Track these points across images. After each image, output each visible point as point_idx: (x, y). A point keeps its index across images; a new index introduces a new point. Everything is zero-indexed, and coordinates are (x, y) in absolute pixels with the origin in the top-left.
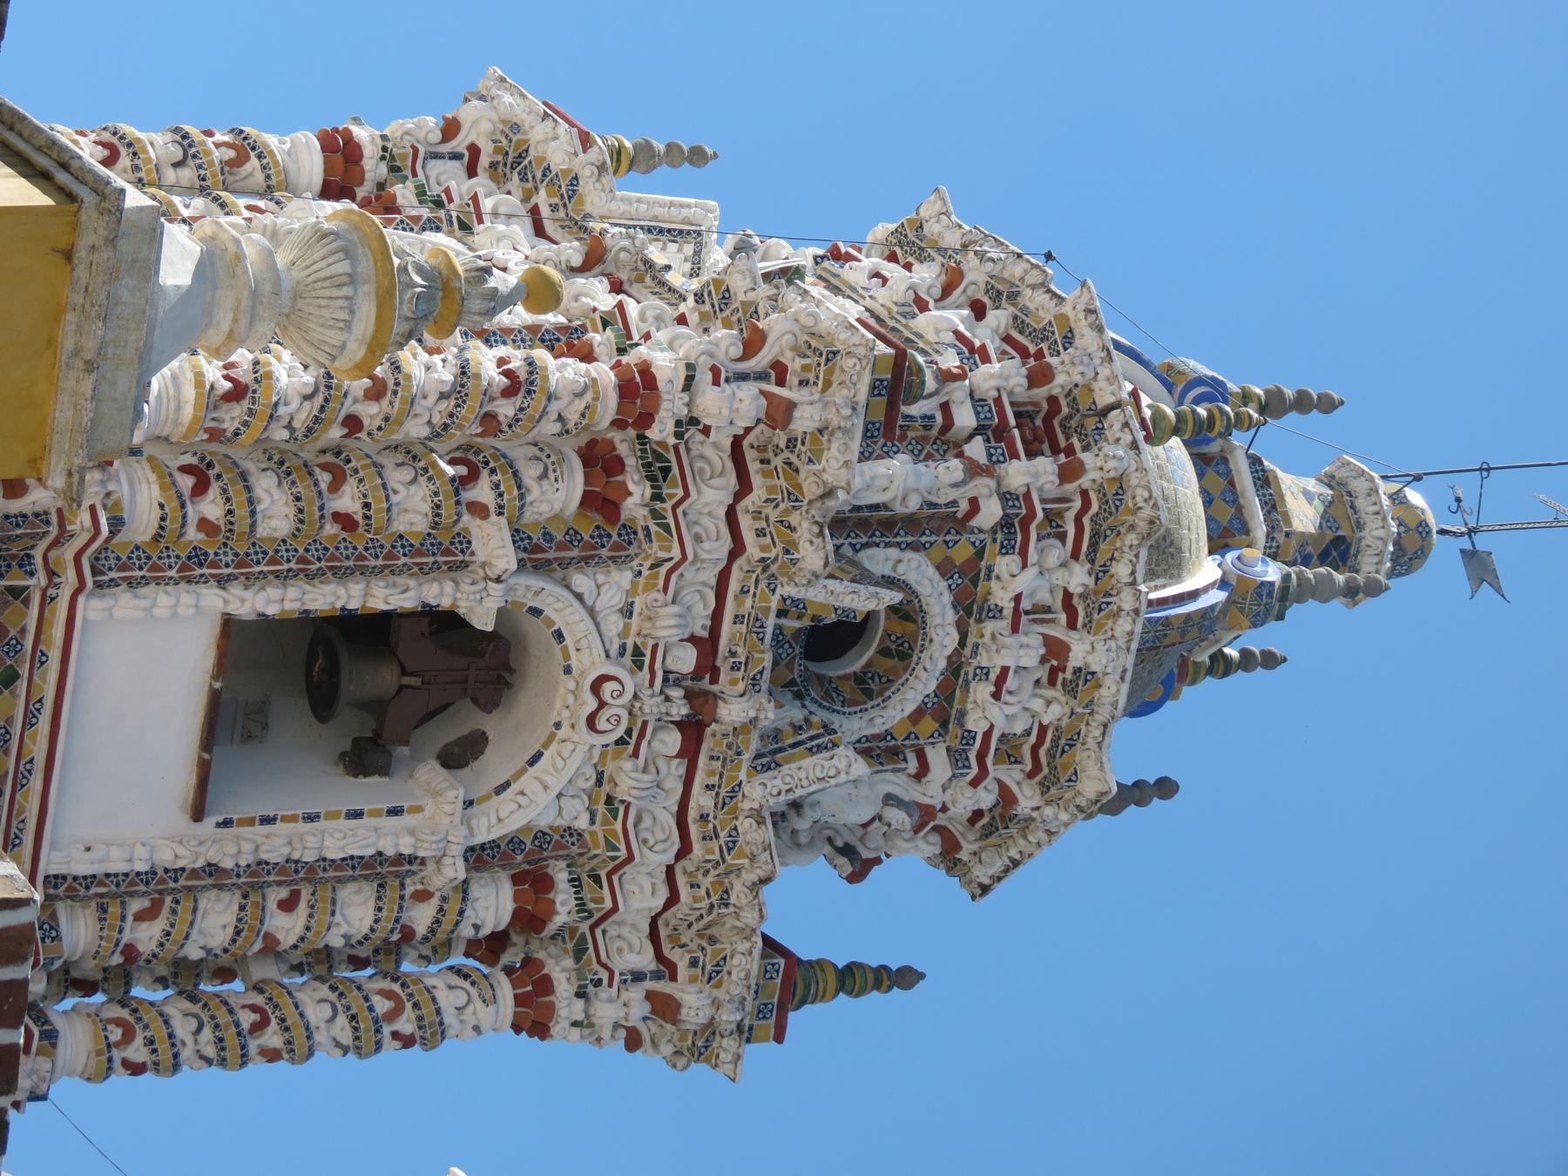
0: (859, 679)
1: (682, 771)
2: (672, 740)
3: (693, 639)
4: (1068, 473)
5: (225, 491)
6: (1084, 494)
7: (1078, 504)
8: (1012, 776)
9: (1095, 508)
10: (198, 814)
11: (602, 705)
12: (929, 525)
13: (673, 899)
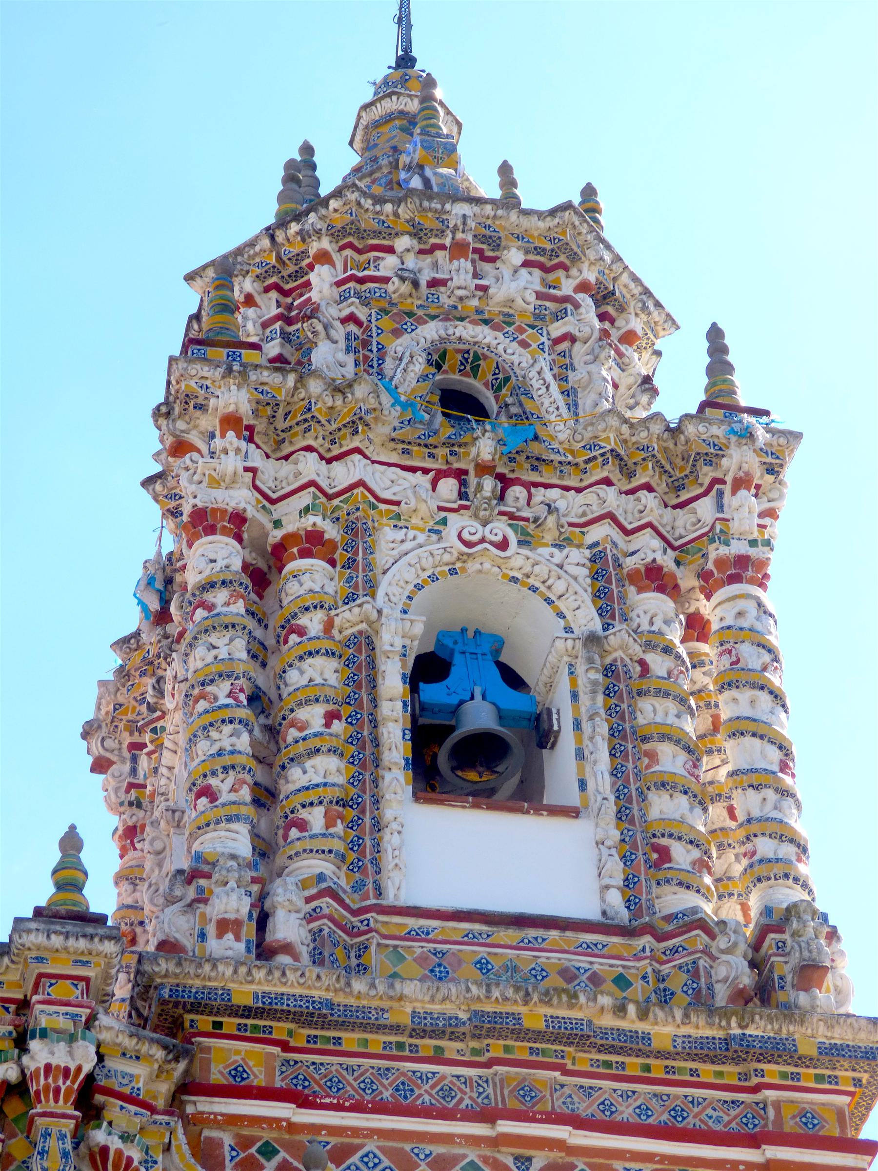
2: (517, 492)
4: (323, 257)
5: (304, 806)
6: (341, 249)
7: (348, 252)
9: (350, 239)
10: (572, 813)
13: (648, 488)
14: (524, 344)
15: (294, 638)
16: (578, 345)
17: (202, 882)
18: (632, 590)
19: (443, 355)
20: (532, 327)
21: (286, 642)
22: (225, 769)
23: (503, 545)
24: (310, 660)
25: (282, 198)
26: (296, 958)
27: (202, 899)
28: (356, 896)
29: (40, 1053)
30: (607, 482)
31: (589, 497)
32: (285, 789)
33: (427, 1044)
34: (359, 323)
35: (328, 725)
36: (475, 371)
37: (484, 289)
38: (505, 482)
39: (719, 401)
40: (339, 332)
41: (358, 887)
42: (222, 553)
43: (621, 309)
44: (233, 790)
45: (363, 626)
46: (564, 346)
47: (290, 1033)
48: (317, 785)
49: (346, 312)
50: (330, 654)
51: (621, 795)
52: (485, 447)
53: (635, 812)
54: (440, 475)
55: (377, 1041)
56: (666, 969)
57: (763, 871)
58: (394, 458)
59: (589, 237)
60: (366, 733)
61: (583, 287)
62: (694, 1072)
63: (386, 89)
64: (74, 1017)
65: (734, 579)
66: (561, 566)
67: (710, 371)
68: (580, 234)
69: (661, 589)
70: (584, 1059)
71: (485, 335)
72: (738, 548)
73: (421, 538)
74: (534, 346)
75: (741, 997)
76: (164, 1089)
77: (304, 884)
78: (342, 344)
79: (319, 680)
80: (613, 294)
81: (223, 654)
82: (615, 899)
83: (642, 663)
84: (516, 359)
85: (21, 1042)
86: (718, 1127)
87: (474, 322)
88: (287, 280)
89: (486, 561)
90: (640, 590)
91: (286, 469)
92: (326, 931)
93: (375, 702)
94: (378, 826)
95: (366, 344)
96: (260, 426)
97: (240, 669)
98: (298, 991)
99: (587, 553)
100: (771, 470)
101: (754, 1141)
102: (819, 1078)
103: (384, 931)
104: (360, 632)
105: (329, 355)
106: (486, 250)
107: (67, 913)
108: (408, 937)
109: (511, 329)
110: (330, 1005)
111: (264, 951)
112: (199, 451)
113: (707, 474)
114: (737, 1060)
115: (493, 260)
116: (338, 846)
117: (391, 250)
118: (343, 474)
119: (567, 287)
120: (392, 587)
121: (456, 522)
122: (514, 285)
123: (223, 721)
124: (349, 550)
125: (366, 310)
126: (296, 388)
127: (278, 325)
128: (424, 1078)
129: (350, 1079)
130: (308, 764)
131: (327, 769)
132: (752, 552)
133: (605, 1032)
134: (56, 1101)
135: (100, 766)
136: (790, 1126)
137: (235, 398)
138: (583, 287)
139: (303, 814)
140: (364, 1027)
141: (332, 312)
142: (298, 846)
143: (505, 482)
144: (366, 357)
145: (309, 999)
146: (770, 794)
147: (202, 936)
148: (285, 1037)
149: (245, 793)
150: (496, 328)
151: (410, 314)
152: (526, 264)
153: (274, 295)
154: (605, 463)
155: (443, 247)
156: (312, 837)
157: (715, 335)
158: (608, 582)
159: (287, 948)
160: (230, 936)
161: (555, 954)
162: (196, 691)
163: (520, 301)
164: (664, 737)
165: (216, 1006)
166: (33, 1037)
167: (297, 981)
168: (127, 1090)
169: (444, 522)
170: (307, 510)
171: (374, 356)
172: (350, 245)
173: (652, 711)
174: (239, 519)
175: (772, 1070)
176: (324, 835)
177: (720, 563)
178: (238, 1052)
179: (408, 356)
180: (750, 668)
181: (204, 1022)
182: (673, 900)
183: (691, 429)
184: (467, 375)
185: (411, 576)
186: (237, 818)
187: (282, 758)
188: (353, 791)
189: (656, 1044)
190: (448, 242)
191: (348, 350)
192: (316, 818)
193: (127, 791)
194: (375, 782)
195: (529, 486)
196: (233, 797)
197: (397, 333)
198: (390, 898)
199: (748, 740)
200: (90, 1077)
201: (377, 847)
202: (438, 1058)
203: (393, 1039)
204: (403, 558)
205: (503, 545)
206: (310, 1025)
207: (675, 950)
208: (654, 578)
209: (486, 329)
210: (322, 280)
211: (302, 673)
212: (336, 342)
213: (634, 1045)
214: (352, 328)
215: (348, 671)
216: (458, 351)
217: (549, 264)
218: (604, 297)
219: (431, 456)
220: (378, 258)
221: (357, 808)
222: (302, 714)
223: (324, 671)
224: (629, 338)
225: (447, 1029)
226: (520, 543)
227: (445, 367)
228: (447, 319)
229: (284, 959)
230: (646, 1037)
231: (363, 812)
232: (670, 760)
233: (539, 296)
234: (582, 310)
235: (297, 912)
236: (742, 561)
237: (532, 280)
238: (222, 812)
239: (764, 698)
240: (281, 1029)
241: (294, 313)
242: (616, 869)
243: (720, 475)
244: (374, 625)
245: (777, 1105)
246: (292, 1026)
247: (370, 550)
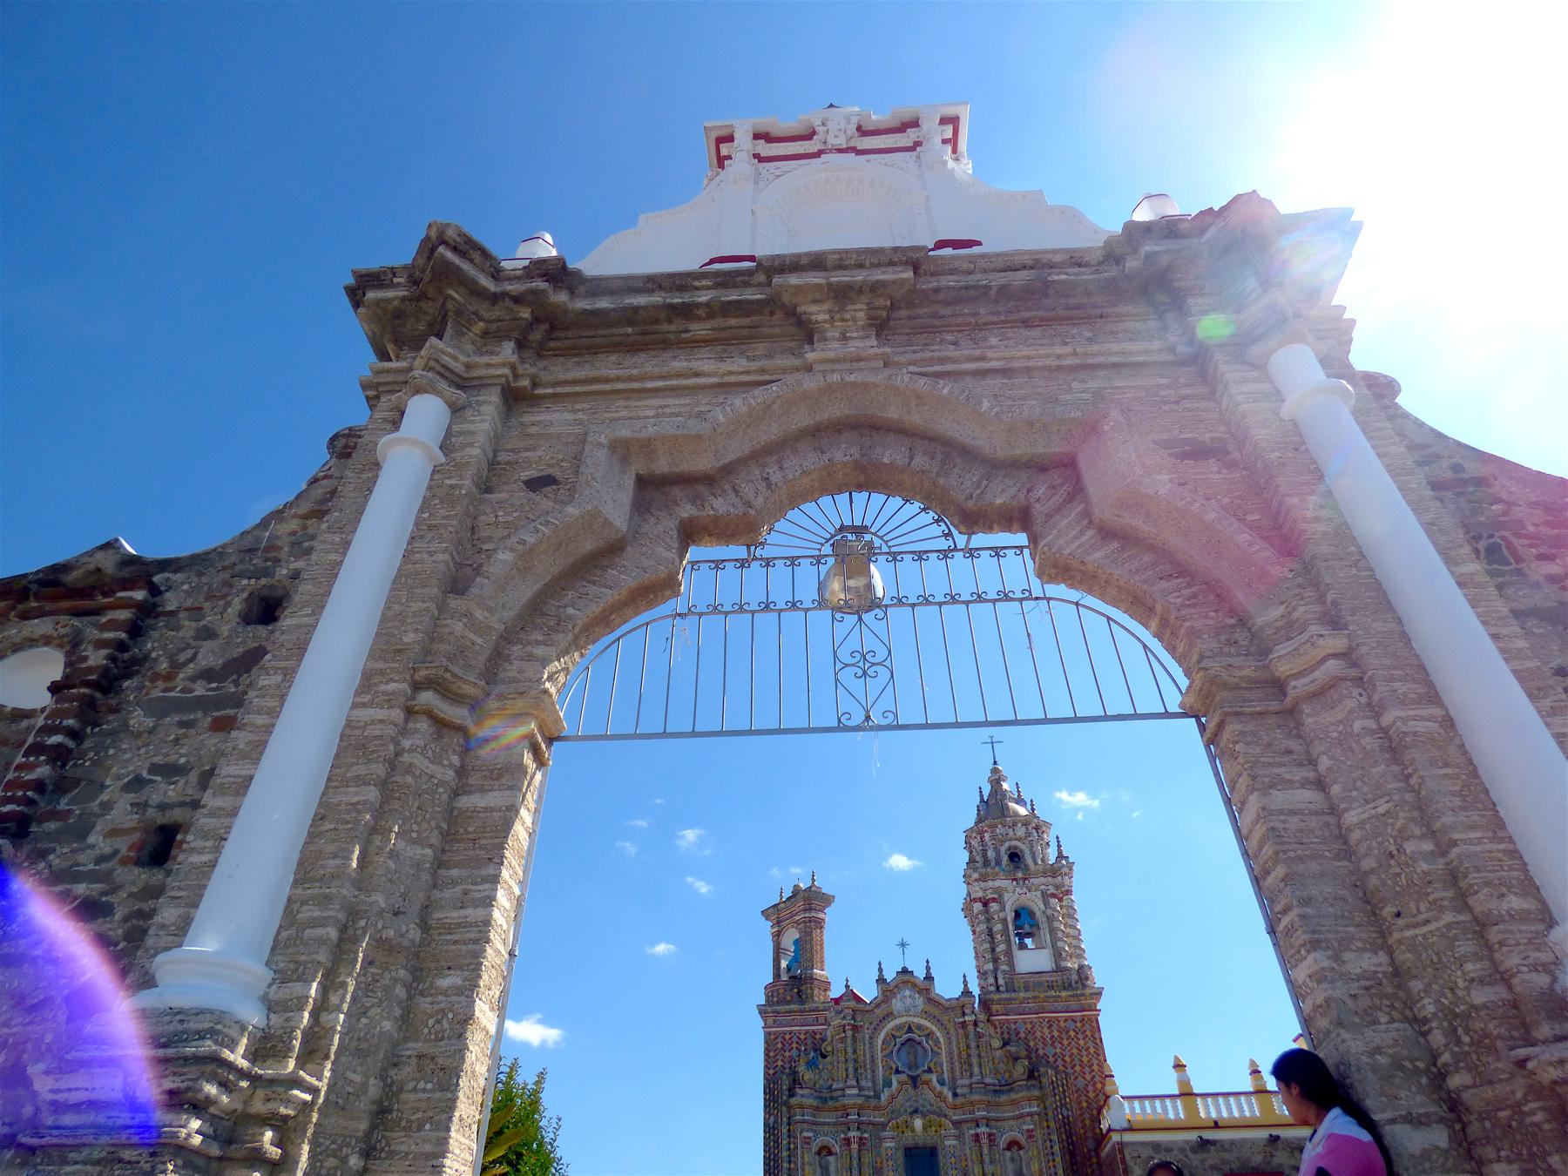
39: (1060, 856)
52: (1020, 875)
85: (964, 1014)
88: (981, 833)
105: (991, 854)
107: (966, 992)
118: (998, 883)
120: (1008, 907)
122: (1021, 831)
124: (999, 900)
137: (976, 876)
158: (1046, 896)
161: (1045, 978)
173: (1056, 924)
179: (1005, 859)
180: (1070, 913)
182: (1063, 964)
208: (1053, 895)
221: (1009, 953)
223: (998, 927)
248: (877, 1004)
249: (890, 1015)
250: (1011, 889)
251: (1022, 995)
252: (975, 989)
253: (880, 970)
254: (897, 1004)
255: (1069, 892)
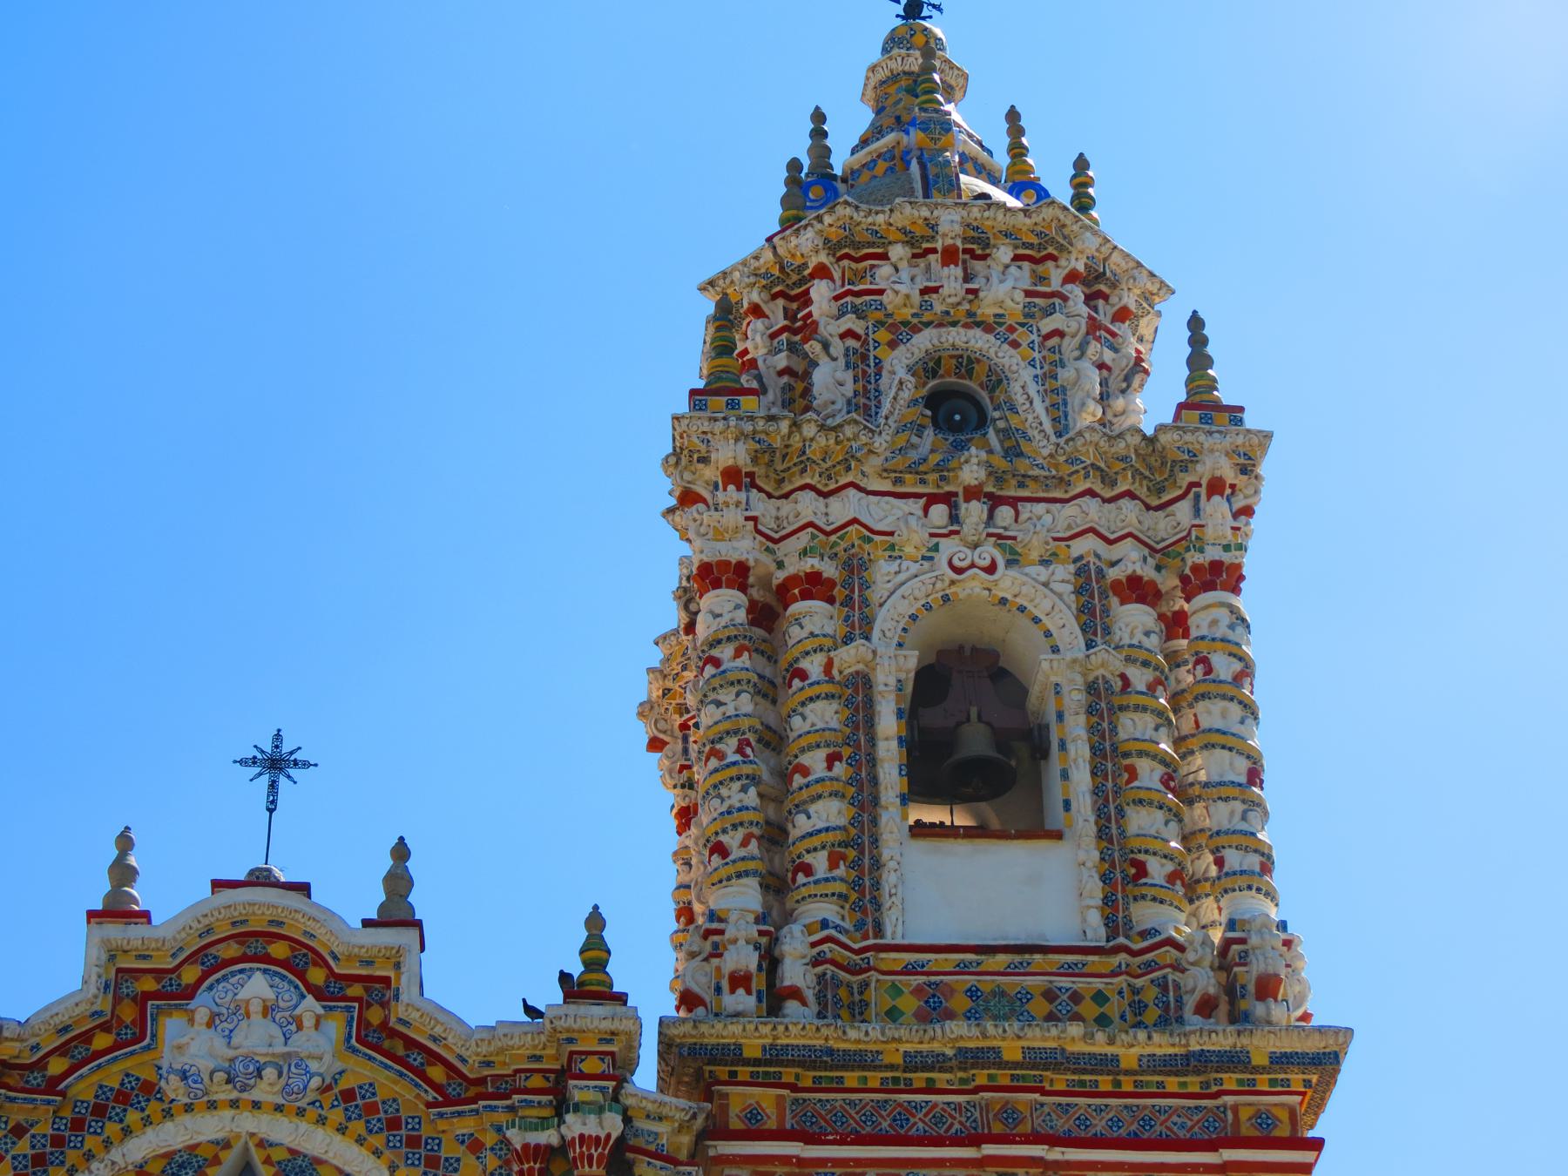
0: (992, 390)
1: (1028, 505)
2: (1005, 513)
3: (926, 510)
4: (822, 272)
6: (840, 259)
7: (846, 262)
8: (1056, 276)
9: (846, 250)
10: (1058, 835)
11: (973, 565)
12: (864, 364)
13: (1130, 494)
14: (1015, 345)
15: (797, 683)
16: (1067, 340)
17: (716, 938)
18: (1114, 601)
19: (938, 361)
20: (1022, 325)
21: (790, 686)
22: (735, 827)
23: (991, 569)
24: (811, 706)
25: (785, 201)
26: (804, 1004)
27: (716, 953)
28: (858, 935)
29: (575, 1125)
30: (1090, 493)
31: (1070, 510)
32: (794, 833)
33: (919, 1078)
34: (856, 336)
35: (830, 768)
36: (970, 373)
37: (975, 292)
38: (995, 501)
40: (838, 348)
41: (860, 925)
42: (725, 605)
43: (1114, 286)
44: (745, 843)
45: (861, 667)
46: (1054, 341)
47: (797, 1076)
48: (820, 831)
49: (842, 330)
50: (829, 697)
51: (1101, 814)
52: (971, 472)
53: (1114, 831)
54: (932, 499)
55: (874, 1079)
56: (1139, 982)
57: (1228, 881)
58: (886, 486)
59: (1075, 228)
60: (864, 774)
61: (1072, 277)
62: (1160, 1084)
63: (893, 41)
64: (602, 1089)
65: (1209, 586)
66: (1046, 585)
67: (1190, 362)
68: (1064, 226)
69: (1141, 600)
70: (1060, 1081)
71: (979, 341)
72: (1213, 553)
73: (914, 568)
74: (1024, 345)
75: (1206, 1007)
76: (686, 1140)
77: (809, 929)
78: (842, 361)
79: (820, 725)
80: (1104, 273)
81: (730, 711)
82: (1095, 919)
83: (1123, 677)
84: (1006, 361)
85: (562, 1106)
86: (1182, 1134)
87: (966, 326)
89: (973, 586)
90: (1123, 603)
91: (786, 507)
92: (829, 974)
93: (872, 740)
94: (877, 864)
95: (864, 358)
96: (759, 471)
97: (745, 723)
98: (802, 1042)
99: (1072, 568)
100: (1244, 470)
101: (1212, 1146)
102: (1273, 1082)
103: (884, 967)
104: (857, 673)
105: (830, 379)
106: (972, 251)
108: (908, 971)
109: (1002, 329)
110: (831, 1052)
111: (775, 999)
112: (704, 501)
113: (1185, 479)
114: (1197, 1072)
115: (984, 257)
116: (840, 887)
117: (884, 257)
118: (842, 508)
119: (1056, 284)
120: (887, 621)
121: (948, 546)
122: (1004, 288)
123: (732, 779)
124: (845, 589)
125: (862, 323)
126: (790, 433)
127: (784, 336)
128: (918, 1107)
129: (852, 1112)
130: (812, 809)
131: (829, 813)
132: (1227, 558)
133: (1078, 1057)
134: (590, 1166)
135: (655, 745)
136: (1246, 1131)
137: (730, 453)
138: (1072, 277)
139: (808, 859)
140: (864, 1068)
141: (831, 329)
142: (804, 891)
143: (995, 501)
144: (864, 372)
145: (810, 1048)
146: (1239, 807)
147: (718, 990)
148: (792, 1080)
149: (753, 846)
150: (988, 328)
151: (905, 323)
152: (1017, 258)
153: (781, 302)
154: (1087, 476)
155: (934, 251)
156: (816, 882)
157: (1196, 323)
158: (1095, 595)
159: (795, 993)
160: (741, 991)
162: (707, 749)
163: (1009, 303)
164: (1141, 754)
165: (731, 1055)
166: (568, 1112)
167: (800, 1026)
168: (652, 1148)
169: (936, 548)
170: (804, 553)
171: (871, 371)
172: (847, 256)
173: (1133, 726)
174: (742, 569)
175: (1230, 1080)
176: (827, 880)
177: (1196, 568)
178: (752, 1096)
181: (722, 1072)
182: (1145, 914)
183: (1164, 439)
184: (962, 377)
185: (907, 608)
186: (747, 873)
187: (788, 805)
188: (853, 831)
189: (1123, 1065)
190: (939, 245)
191: (847, 366)
192: (820, 861)
193: (680, 771)
194: (874, 822)
195: (1013, 502)
196: (743, 853)
197: (893, 345)
198: (888, 940)
199: (1218, 751)
200: (621, 1139)
201: (877, 885)
202: (930, 1089)
203: (889, 1074)
204: (901, 592)
205: (991, 569)
206: (814, 1069)
207: (1148, 964)
208: (1137, 590)
209: (978, 332)
210: (821, 291)
211: (804, 718)
212: (834, 359)
213: (1107, 1064)
214: (851, 343)
215: (847, 712)
216: (952, 357)
217: (1038, 256)
218: (1096, 282)
219: (923, 482)
220: (873, 267)
221: (858, 850)
222: (805, 759)
223: (825, 715)
224: (1123, 315)
225: (938, 1062)
226: (1010, 563)
227: (941, 372)
228: (940, 325)
229: (792, 1006)
230: (1115, 1059)
231: (862, 852)
232: (1149, 774)
233: (1028, 294)
234: (1071, 303)
235: (804, 957)
236: (1216, 566)
237: (1022, 276)
238: (731, 870)
239: (1235, 710)
240: (789, 1074)
241: (799, 324)
242: (1095, 889)
243: (1194, 479)
244: (871, 664)
245: (1235, 1109)
246: (798, 1070)
247: (866, 585)
248: (76, 1042)
249: (140, 1096)
250: (914, 535)
251: (910, 1039)
252: (649, 978)
253: (123, 873)
254: (187, 1042)
255: (1225, 576)
